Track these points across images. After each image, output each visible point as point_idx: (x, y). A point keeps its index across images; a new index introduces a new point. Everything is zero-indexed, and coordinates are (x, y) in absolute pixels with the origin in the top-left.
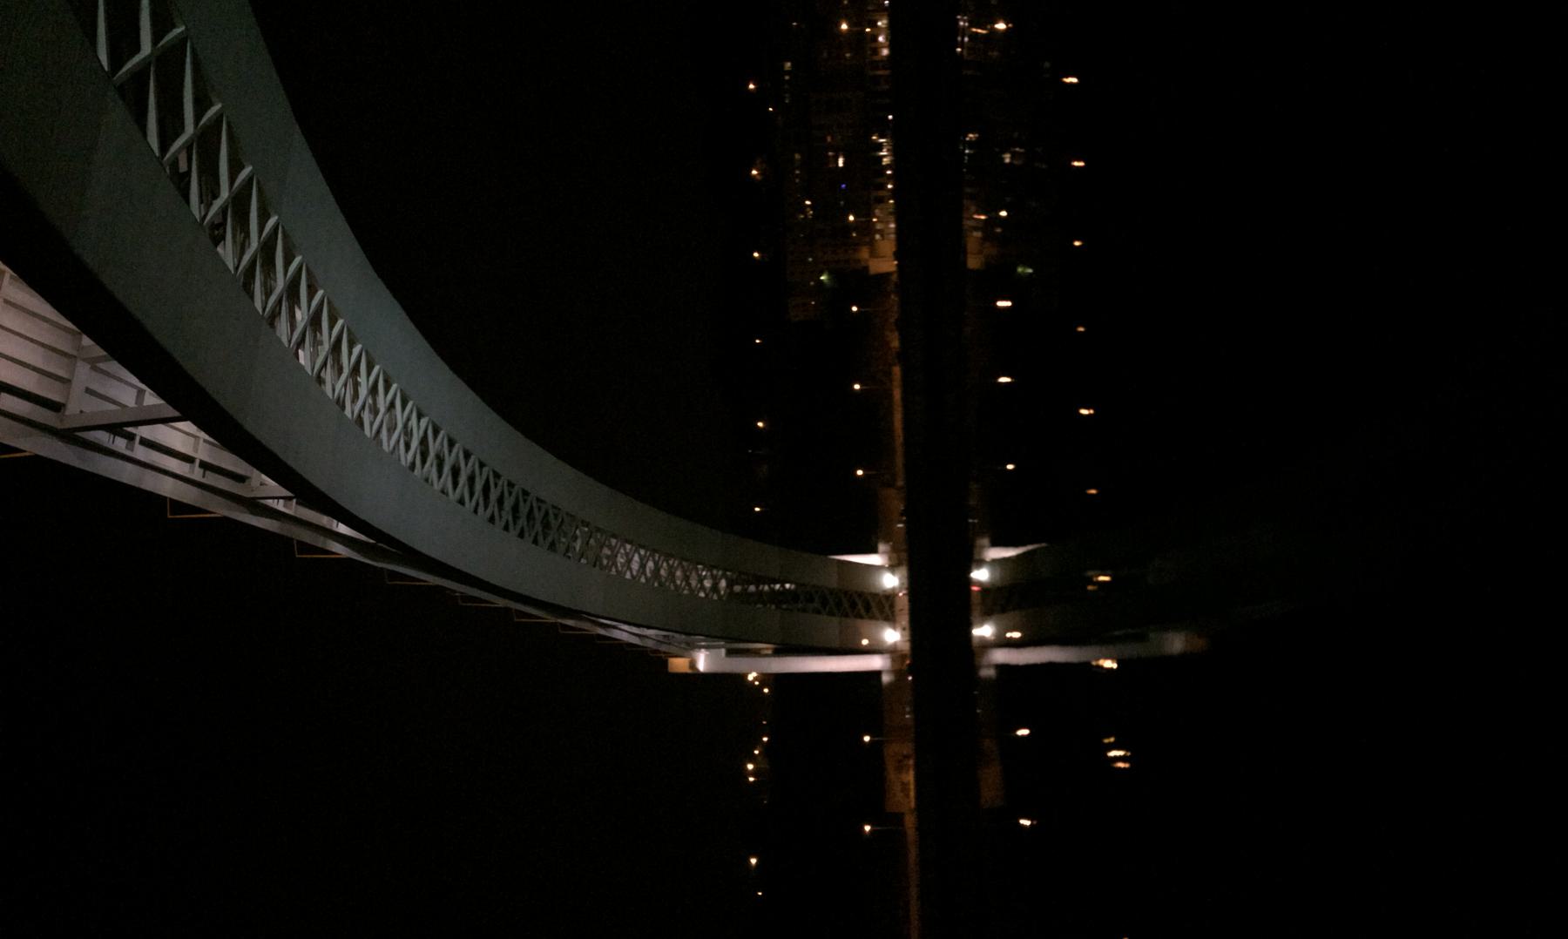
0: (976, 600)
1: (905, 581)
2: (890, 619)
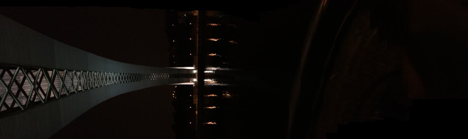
0: (197, 76)
2: (195, 77)
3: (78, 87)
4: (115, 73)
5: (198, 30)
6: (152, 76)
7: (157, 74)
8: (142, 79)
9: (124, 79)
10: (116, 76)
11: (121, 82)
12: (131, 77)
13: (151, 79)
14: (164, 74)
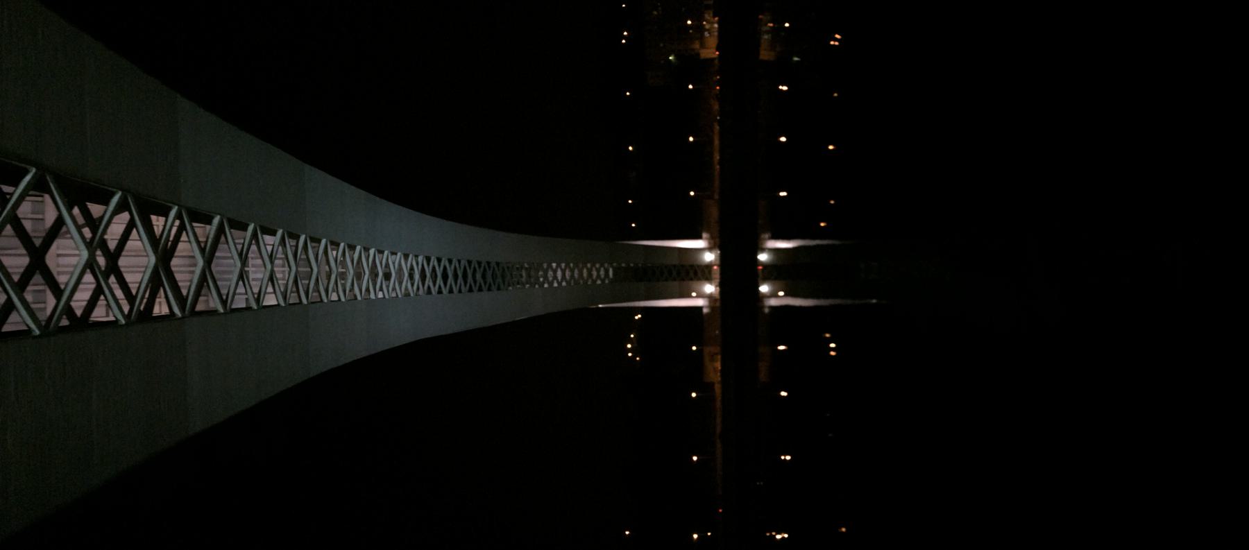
1: (718, 258)
2: (709, 279)
3: (263, 289)
4: (406, 256)
5: (716, 107)
8: (509, 286)
10: (412, 269)
11: (429, 292)
12: (470, 273)
13: (546, 286)
14: (593, 265)
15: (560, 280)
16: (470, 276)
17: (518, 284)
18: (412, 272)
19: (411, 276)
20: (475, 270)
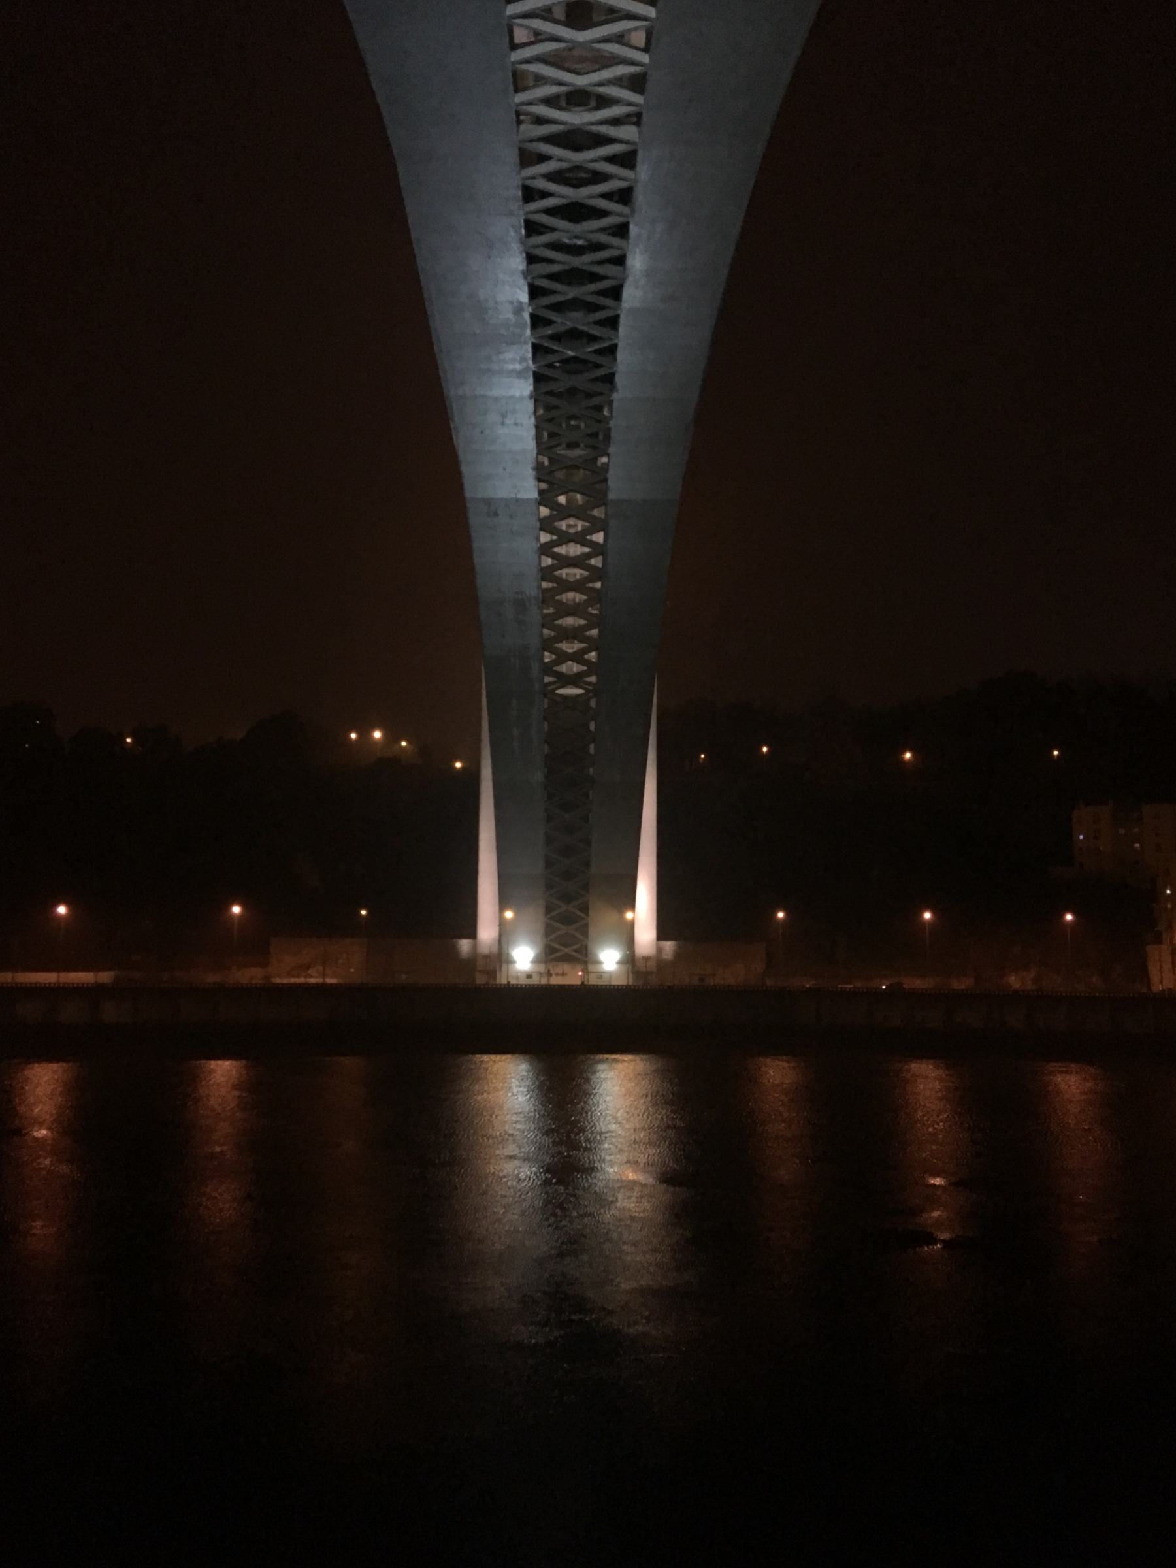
1: (604, 982)
2: (549, 955)
4: (637, 83)
6: (580, 525)
7: (596, 574)
9: (565, 194)
10: (604, 102)
12: (585, 291)
14: (593, 645)
15: (556, 550)
16: (571, 292)
17: (552, 435)
18: (593, 104)
19: (578, 98)
20: (592, 308)
